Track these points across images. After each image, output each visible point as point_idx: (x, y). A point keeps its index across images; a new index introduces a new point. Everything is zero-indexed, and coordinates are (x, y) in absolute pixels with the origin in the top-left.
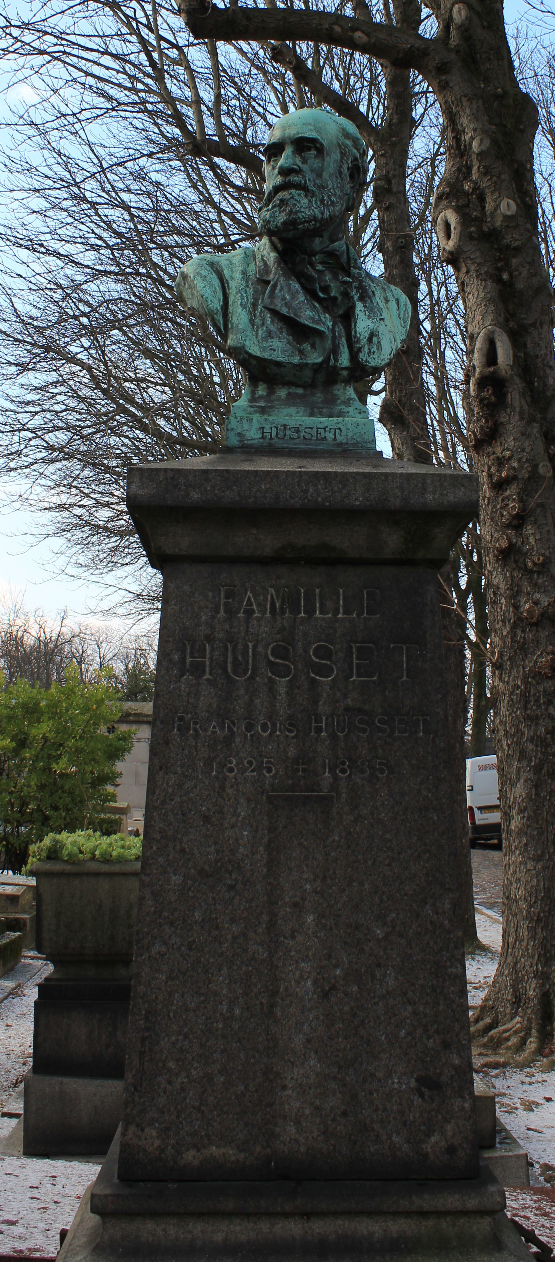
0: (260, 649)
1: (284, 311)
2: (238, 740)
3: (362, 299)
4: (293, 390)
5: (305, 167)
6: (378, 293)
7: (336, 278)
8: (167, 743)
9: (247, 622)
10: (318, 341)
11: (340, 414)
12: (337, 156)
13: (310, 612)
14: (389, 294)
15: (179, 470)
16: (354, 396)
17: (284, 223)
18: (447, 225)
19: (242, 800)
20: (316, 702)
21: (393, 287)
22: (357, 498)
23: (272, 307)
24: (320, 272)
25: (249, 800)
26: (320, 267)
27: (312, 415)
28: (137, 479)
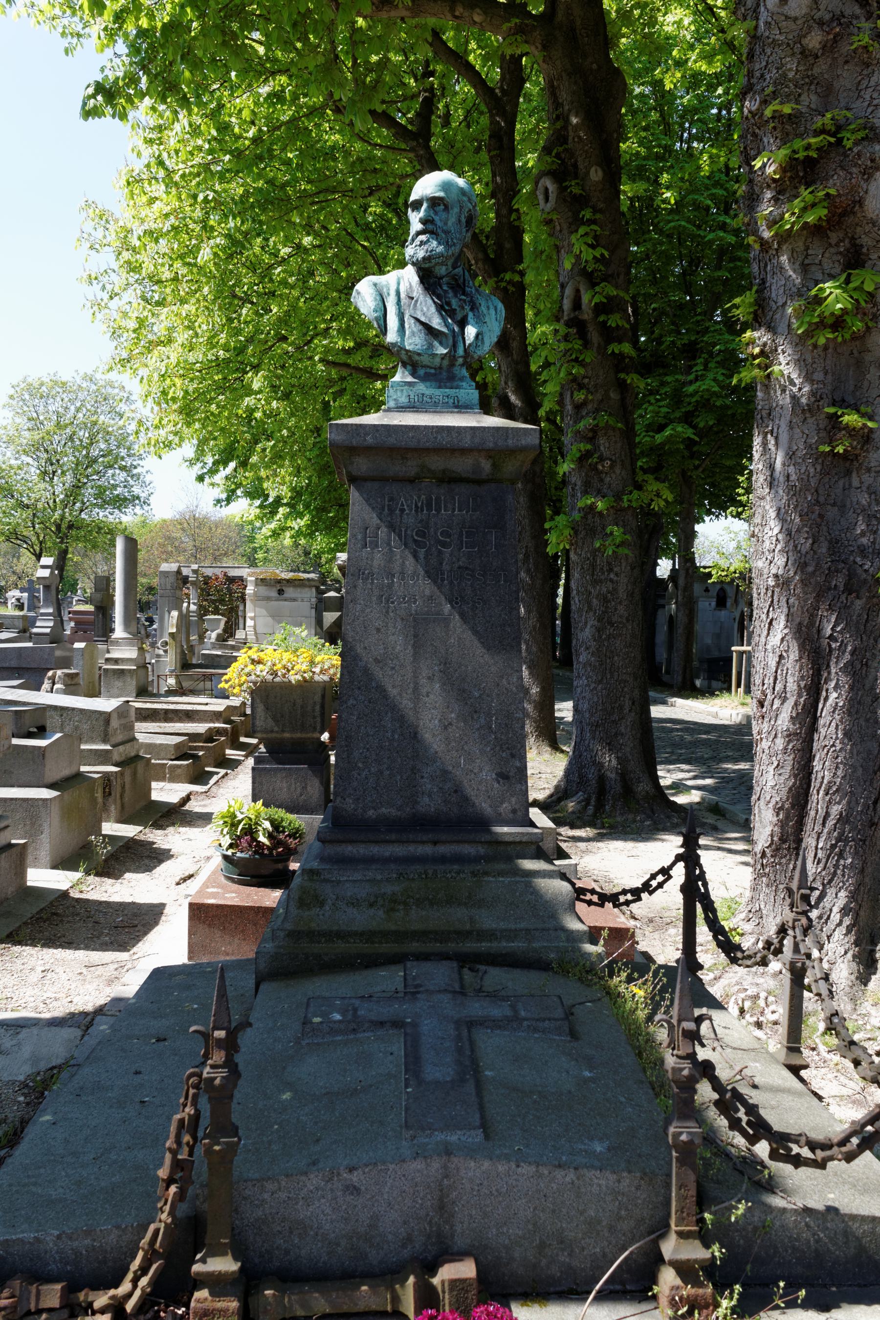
0: (409, 532)
1: (423, 319)
3: (472, 309)
4: (428, 370)
5: (436, 218)
6: (483, 303)
7: (456, 296)
8: (355, 587)
10: (444, 340)
11: (458, 387)
12: (457, 210)
13: (438, 510)
14: (490, 304)
15: (360, 425)
16: (467, 375)
17: (424, 258)
18: (546, 189)
20: (441, 564)
21: (493, 298)
22: (467, 442)
24: (445, 291)
26: (445, 288)
27: (440, 387)
28: (334, 430)
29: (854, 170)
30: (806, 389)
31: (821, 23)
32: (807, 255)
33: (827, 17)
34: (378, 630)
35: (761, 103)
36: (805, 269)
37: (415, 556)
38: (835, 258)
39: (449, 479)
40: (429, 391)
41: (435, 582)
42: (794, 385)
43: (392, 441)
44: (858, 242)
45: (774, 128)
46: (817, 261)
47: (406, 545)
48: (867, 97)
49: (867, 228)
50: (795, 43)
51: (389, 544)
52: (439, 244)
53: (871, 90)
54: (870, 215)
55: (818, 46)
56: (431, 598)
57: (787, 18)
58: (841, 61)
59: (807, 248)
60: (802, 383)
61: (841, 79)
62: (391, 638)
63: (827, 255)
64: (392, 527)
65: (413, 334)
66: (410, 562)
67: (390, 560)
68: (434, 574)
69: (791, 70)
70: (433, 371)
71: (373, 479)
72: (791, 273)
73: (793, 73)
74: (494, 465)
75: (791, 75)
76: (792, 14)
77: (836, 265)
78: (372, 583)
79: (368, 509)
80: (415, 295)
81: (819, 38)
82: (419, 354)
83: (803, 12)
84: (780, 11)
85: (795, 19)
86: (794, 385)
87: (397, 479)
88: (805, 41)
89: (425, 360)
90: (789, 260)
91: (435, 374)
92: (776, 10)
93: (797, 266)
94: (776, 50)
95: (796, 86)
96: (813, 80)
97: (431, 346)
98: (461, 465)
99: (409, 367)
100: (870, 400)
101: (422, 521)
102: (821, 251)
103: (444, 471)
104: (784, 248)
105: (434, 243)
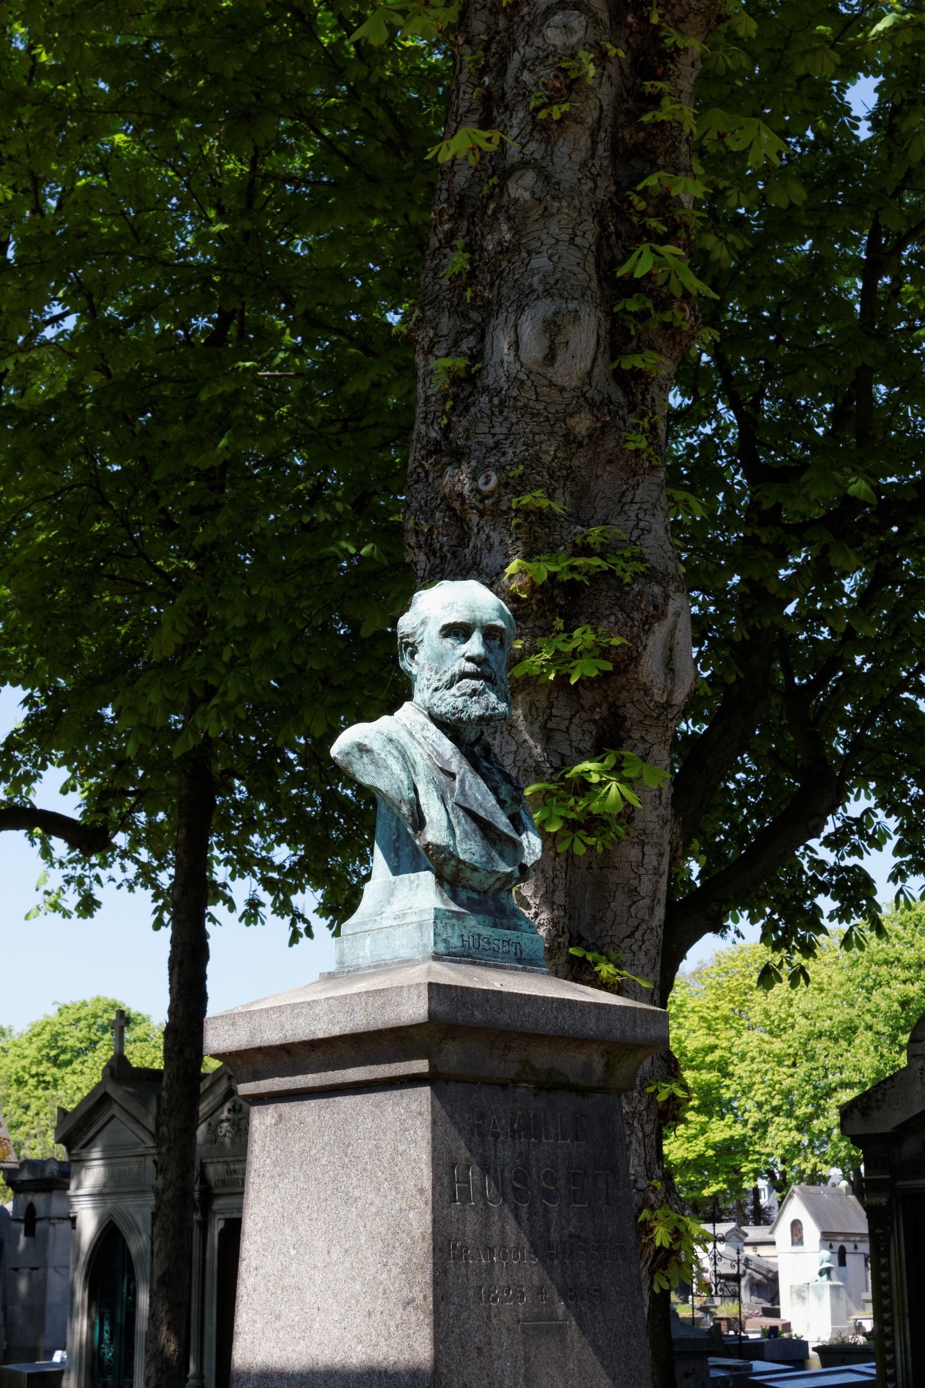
2: (497, 1268)
9: (495, 1146)
17: (481, 718)
19: (504, 1331)
20: (549, 1229)
22: (591, 1027)
23: (467, 806)
25: (509, 1330)
27: (495, 926)
29: (636, 615)
30: (544, 916)
31: (592, 404)
32: (551, 716)
33: (598, 398)
34: (479, 1349)
35: (499, 484)
36: (547, 736)
37: (517, 1217)
38: (586, 726)
39: (551, 1084)
40: (486, 932)
41: (543, 1261)
42: (528, 907)
43: (504, 1018)
44: (621, 711)
45: (518, 526)
46: (563, 727)
47: (503, 1195)
48: (633, 515)
49: (637, 696)
50: (557, 420)
51: (483, 1195)
52: (500, 699)
53: (636, 507)
54: (643, 680)
55: (584, 433)
56: (540, 1291)
57: (552, 384)
58: (604, 457)
59: (551, 706)
60: (538, 906)
61: (601, 482)
62: (496, 1364)
63: (576, 721)
64: (485, 1168)
65: (466, 834)
66: (511, 1227)
67: (486, 1225)
68: (542, 1249)
69: (547, 452)
70: (475, 896)
71: (459, 1080)
72: (527, 737)
73: (550, 458)
74: (608, 1066)
75: (547, 459)
76: (559, 381)
77: (587, 738)
78: (467, 1263)
79: (454, 1132)
80: (454, 768)
81: (588, 423)
82: (475, 869)
83: (574, 384)
84: (541, 371)
85: (562, 390)
86: (528, 907)
87: (488, 1082)
88: (571, 422)
89: (475, 879)
90: (525, 717)
91: (479, 903)
92: (535, 368)
93: (536, 729)
94: (527, 418)
95: (551, 476)
96: (571, 475)
97: (491, 859)
98: (569, 1063)
99: (447, 887)
100: (616, 941)
101: (521, 1154)
102: (568, 714)
103: (550, 1071)
104: (520, 698)
105: (493, 697)
